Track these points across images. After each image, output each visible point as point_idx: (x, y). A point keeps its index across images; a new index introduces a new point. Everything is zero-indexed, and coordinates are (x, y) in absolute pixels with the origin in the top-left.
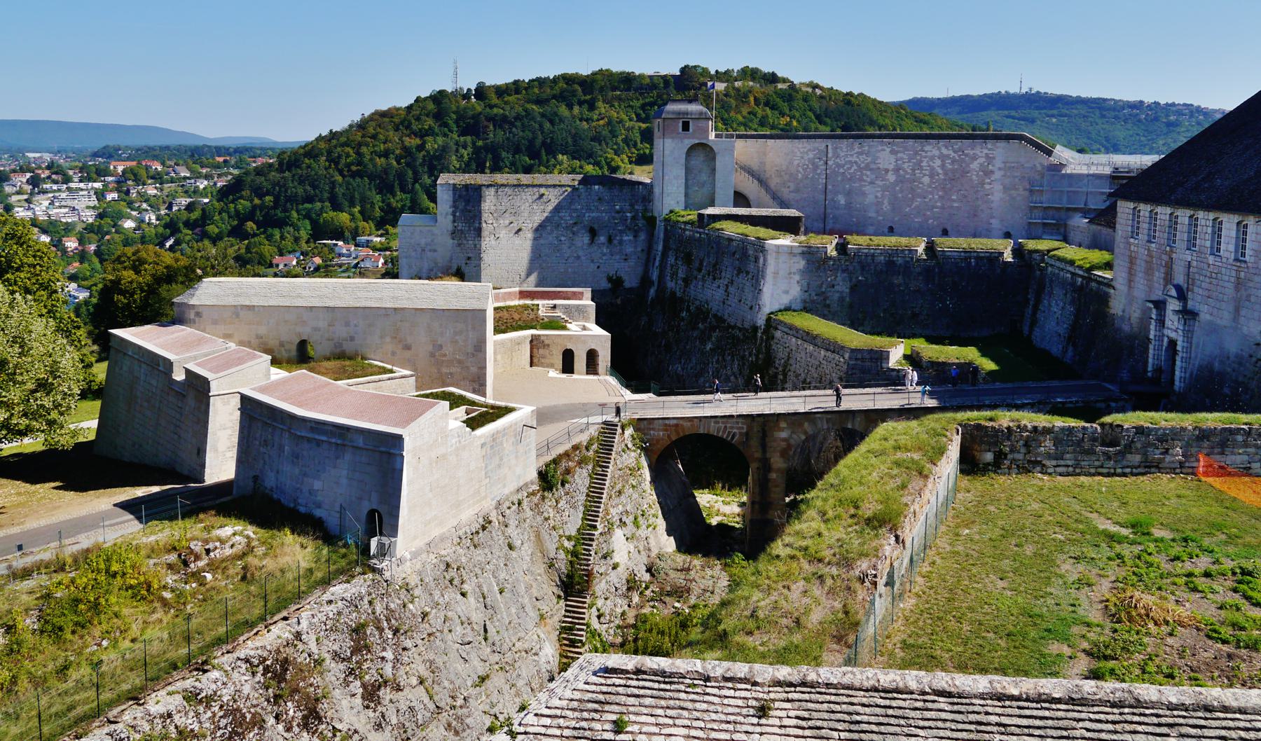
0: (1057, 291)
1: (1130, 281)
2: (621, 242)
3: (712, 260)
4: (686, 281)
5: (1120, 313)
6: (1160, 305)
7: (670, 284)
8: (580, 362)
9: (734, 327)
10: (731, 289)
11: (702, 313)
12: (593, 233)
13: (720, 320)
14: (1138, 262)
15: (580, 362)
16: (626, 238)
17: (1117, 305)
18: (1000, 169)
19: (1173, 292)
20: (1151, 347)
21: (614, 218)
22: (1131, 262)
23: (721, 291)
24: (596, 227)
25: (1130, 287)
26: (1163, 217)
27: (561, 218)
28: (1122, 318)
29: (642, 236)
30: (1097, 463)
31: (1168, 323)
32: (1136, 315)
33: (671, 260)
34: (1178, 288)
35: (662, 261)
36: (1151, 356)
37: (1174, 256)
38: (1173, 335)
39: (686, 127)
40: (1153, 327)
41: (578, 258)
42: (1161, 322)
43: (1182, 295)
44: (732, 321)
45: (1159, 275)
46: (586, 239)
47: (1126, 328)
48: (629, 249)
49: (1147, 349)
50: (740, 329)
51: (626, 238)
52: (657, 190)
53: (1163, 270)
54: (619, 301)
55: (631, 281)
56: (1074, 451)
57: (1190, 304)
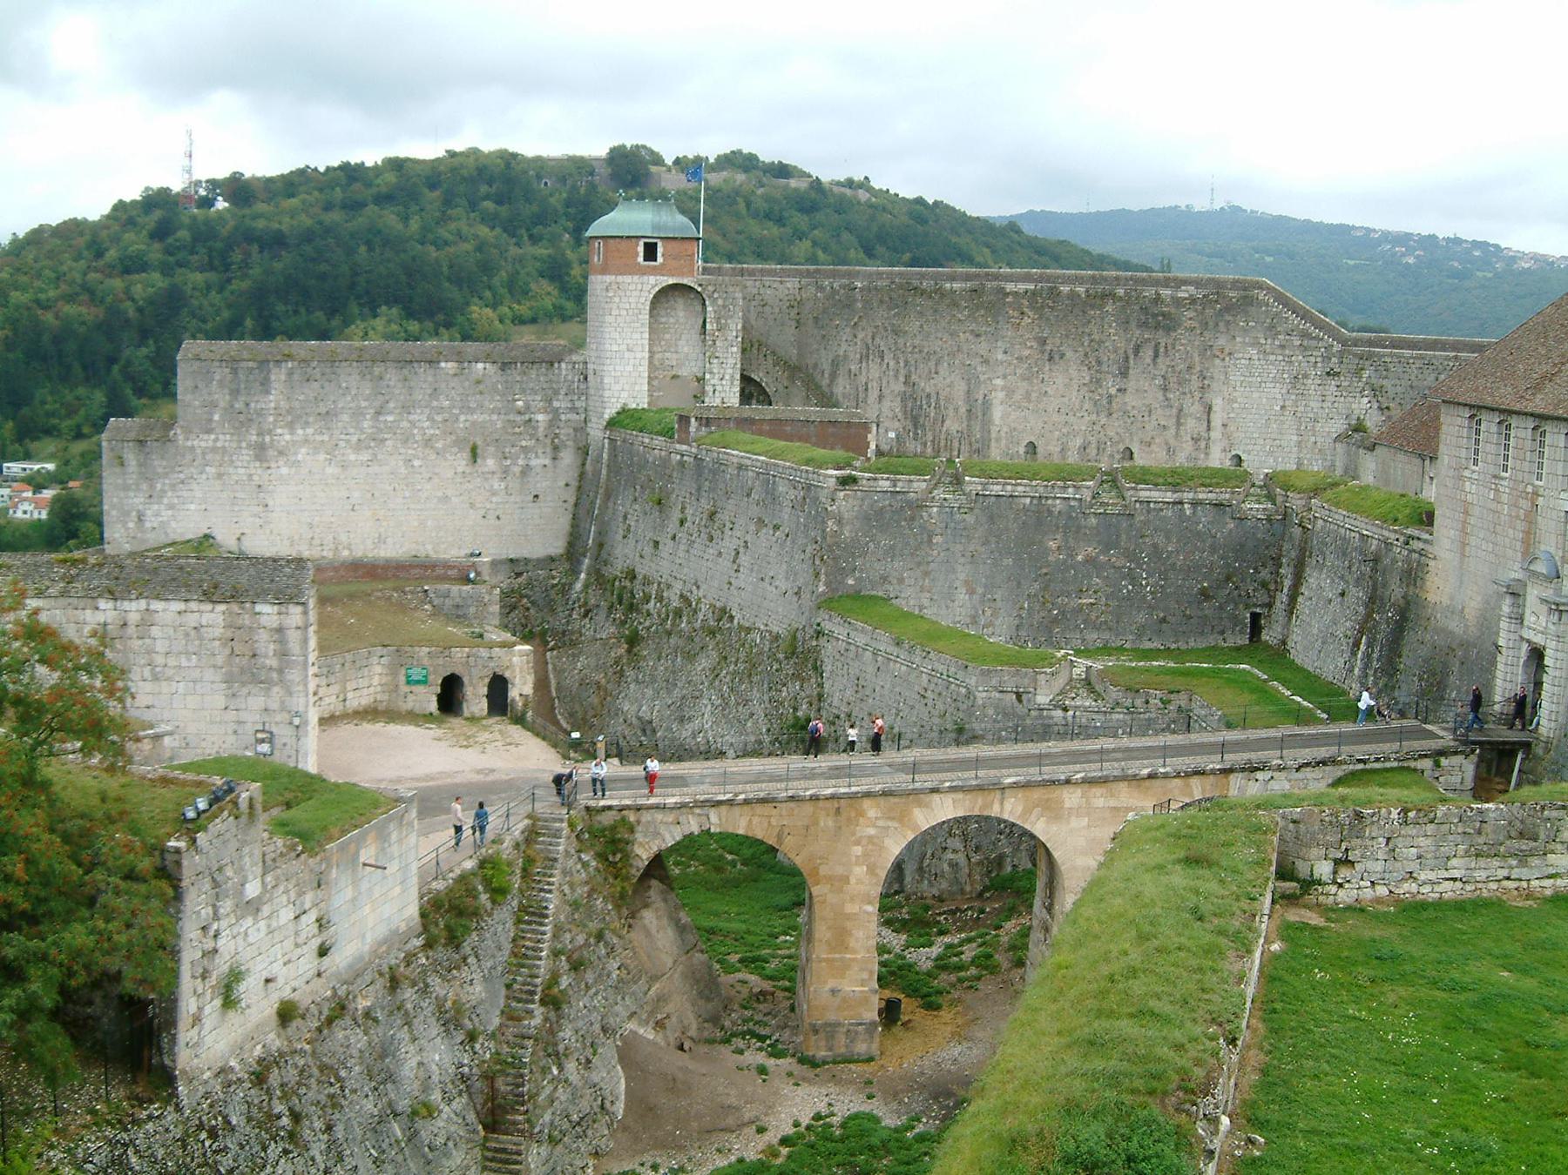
3: (706, 505)
5: (1446, 601)
8: (476, 699)
10: (744, 559)
14: (1476, 511)
15: (476, 699)
16: (533, 463)
23: (725, 563)
27: (413, 424)
29: (568, 457)
30: (1502, 873)
31: (1529, 619)
32: (1473, 604)
36: (1499, 674)
37: (1540, 501)
38: (1538, 639)
40: (1503, 625)
41: (445, 499)
47: (1454, 625)
48: (541, 484)
49: (1493, 663)
53: (1520, 525)
56: (1467, 854)
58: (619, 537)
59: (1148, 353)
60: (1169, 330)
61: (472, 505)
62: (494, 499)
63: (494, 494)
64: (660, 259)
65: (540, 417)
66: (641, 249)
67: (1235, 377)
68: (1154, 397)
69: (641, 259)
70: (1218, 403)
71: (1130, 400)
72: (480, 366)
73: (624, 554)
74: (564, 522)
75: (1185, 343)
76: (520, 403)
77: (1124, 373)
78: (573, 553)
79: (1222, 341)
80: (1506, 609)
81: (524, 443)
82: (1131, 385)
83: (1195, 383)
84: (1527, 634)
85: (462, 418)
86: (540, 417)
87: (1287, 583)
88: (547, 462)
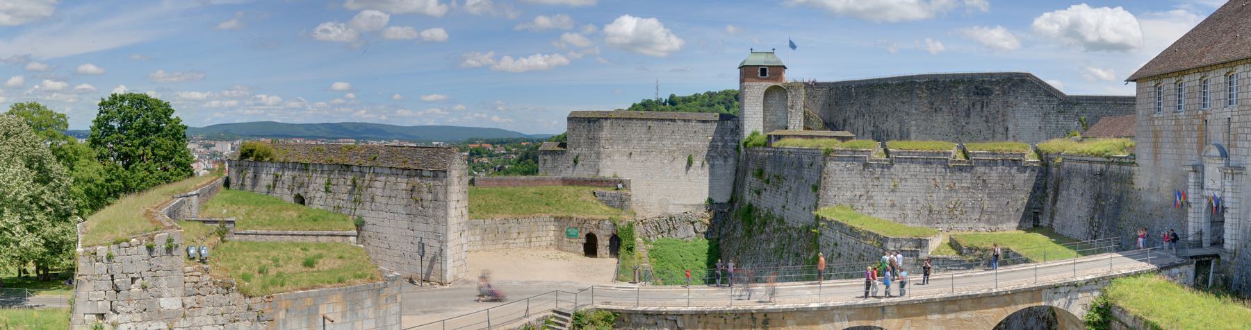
0: (1077, 182)
1: (1156, 154)
5: (1146, 186)
6: (1198, 170)
17: (1142, 180)
19: (1215, 152)
20: (1190, 210)
22: (1156, 136)
25: (1156, 159)
26: (1192, 84)
28: (1150, 191)
29: (731, 161)
34: (1220, 147)
37: (1208, 117)
42: (1201, 186)
43: (1224, 154)
45: (1190, 142)
47: (1154, 198)
57: (1233, 160)
59: (978, 107)
60: (988, 95)
67: (1018, 115)
68: (982, 125)
70: (1011, 127)
71: (971, 127)
73: (748, 197)
74: (729, 189)
75: (996, 102)
77: (968, 116)
78: (732, 202)
79: (1012, 99)
80: (1191, 180)
82: (971, 121)
83: (1000, 119)
84: (1206, 193)
87: (1051, 196)
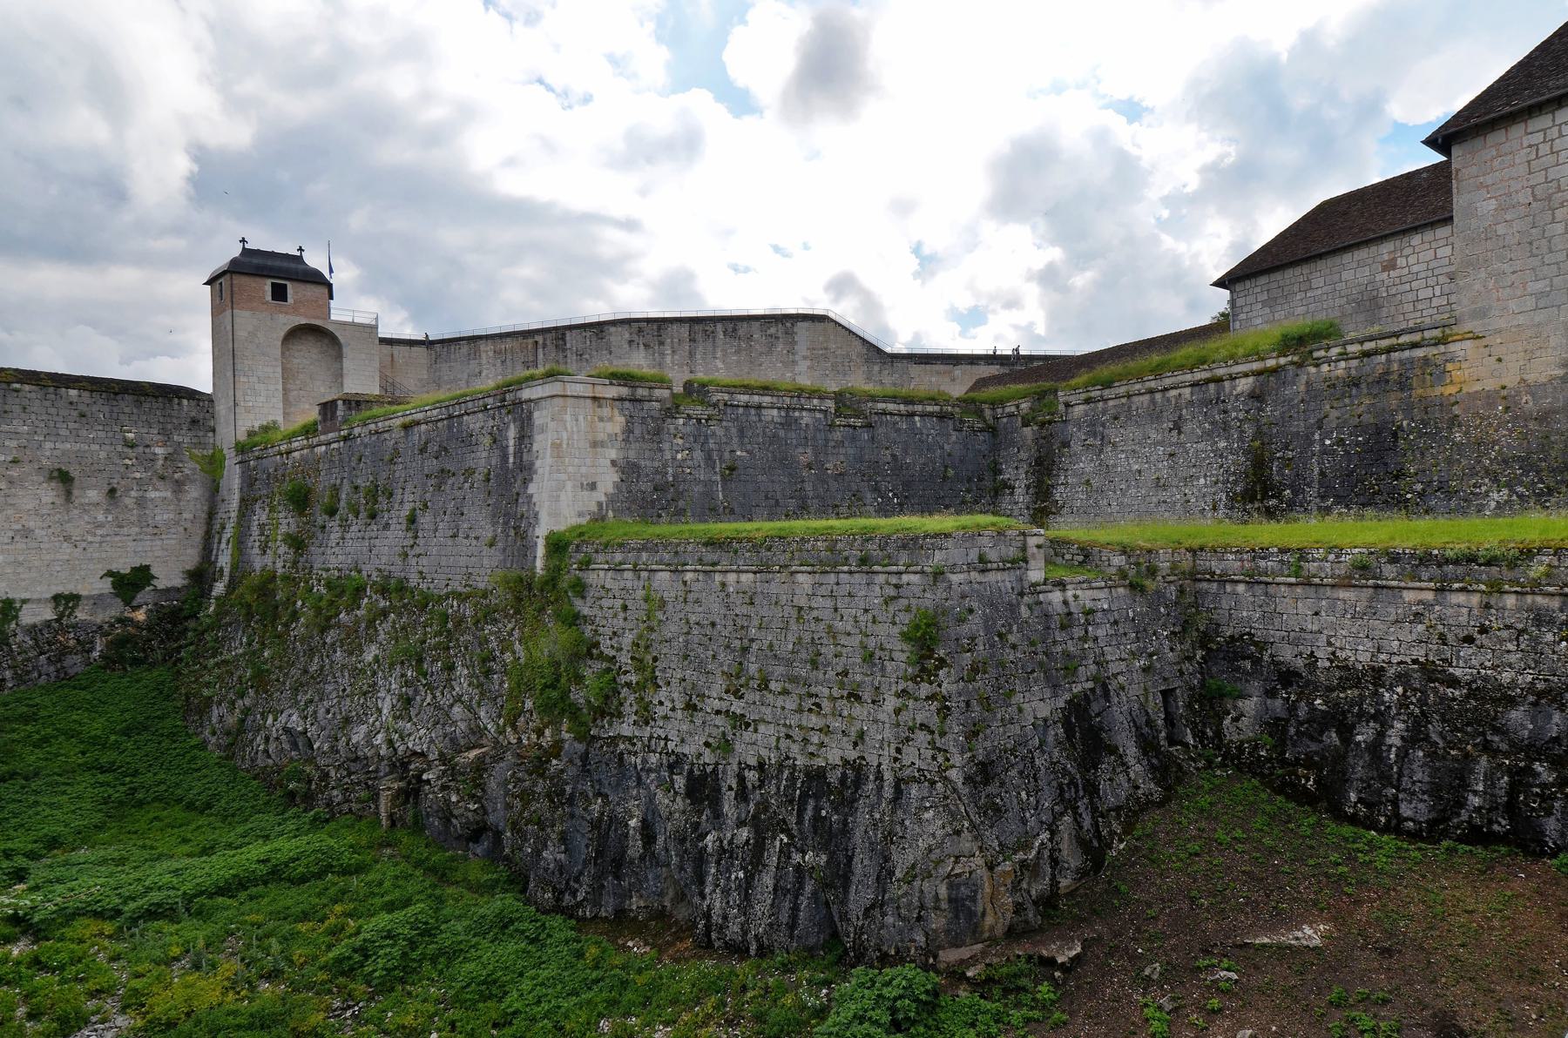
2: (141, 503)
4: (298, 544)
7: (258, 562)
9: (440, 599)
10: (425, 520)
11: (347, 590)
12: (63, 478)
13: (392, 588)
18: (805, 358)
21: (122, 456)
24: (74, 472)
29: (194, 492)
33: (260, 515)
35: (239, 524)
39: (279, 293)
44: (438, 586)
46: (49, 494)
48: (163, 516)
50: (462, 598)
51: (152, 494)
52: (222, 408)
54: (140, 616)
55: (169, 575)
58: (256, 551)
61: (67, 538)
62: (99, 532)
63: (101, 526)
64: (290, 300)
65: (159, 451)
66: (268, 288)
69: (269, 297)
72: (73, 393)
76: (131, 435)
81: (138, 475)
85: (48, 445)
86: (159, 451)
88: (168, 494)
